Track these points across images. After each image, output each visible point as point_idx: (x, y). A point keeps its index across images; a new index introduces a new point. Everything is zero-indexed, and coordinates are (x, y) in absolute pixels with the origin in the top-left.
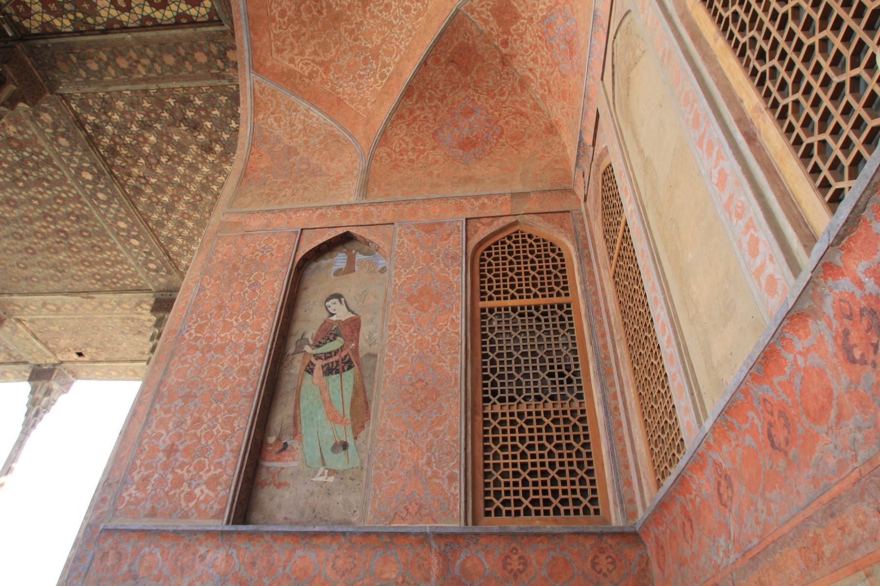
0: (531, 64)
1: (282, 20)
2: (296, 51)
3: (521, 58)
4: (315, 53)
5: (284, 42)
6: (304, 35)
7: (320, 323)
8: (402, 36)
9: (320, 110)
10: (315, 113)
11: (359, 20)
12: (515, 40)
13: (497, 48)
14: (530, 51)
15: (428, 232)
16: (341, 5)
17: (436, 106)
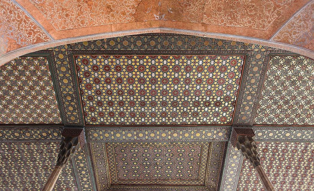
1: (252, 23)
2: (266, 20)
4: (269, 11)
6: (260, 15)
9: (298, 11)
10: (297, 15)
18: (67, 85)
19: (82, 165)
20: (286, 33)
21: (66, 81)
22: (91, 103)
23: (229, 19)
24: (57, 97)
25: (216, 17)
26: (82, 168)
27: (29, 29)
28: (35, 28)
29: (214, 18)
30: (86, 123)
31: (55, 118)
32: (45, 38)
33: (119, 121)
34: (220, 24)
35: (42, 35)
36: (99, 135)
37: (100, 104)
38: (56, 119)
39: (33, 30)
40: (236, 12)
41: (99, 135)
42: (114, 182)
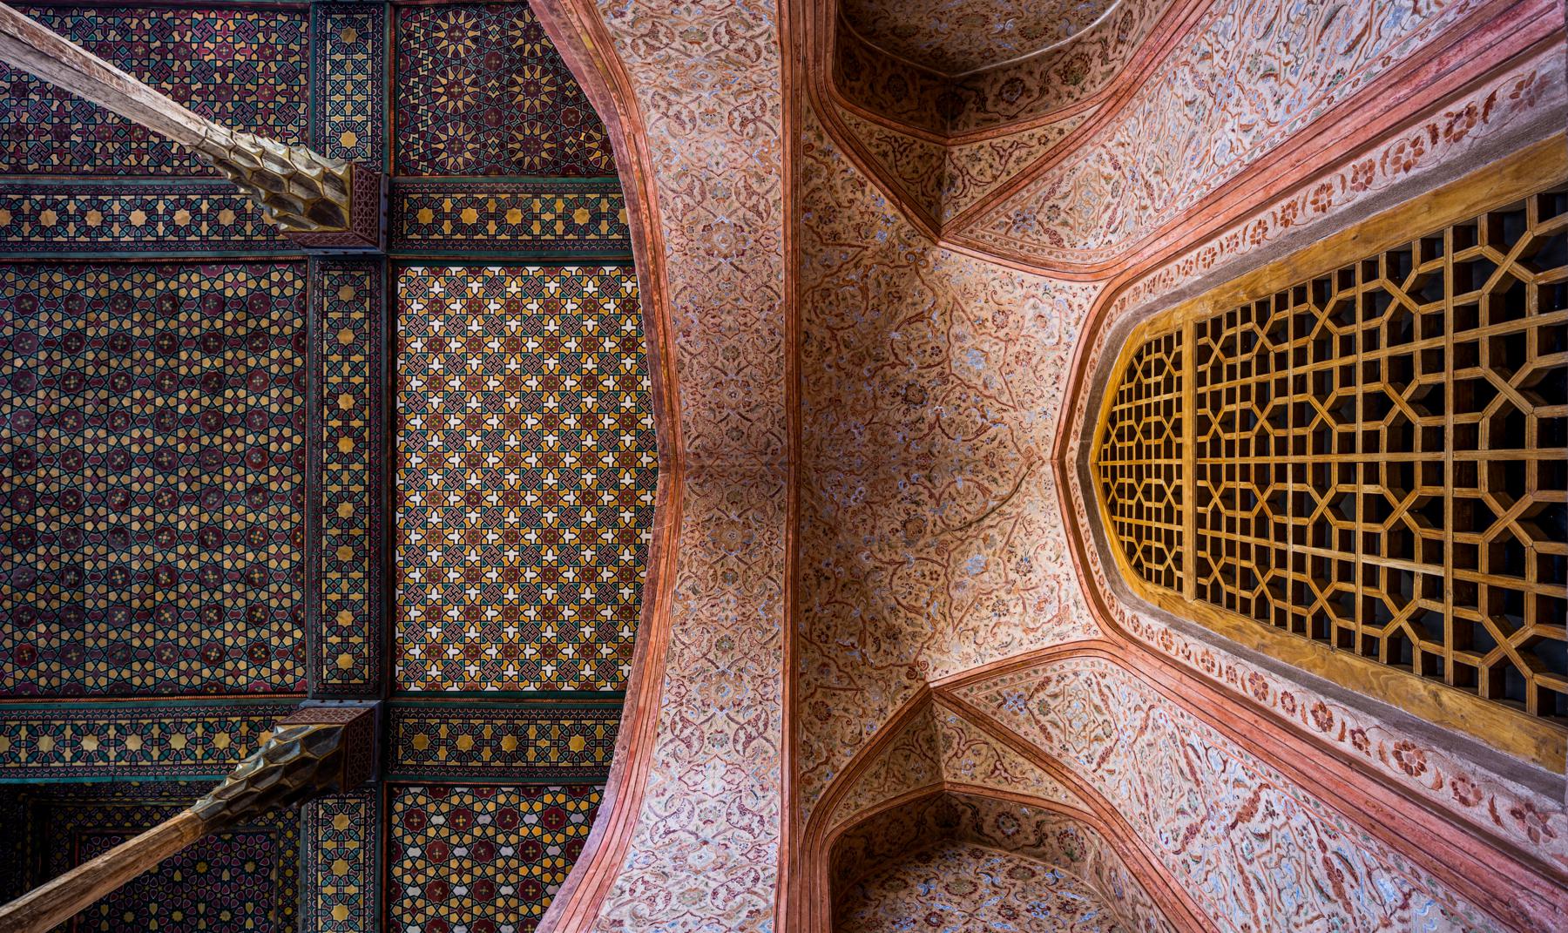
18: (561, 745)
19: (178, 742)
21: (576, 744)
22: (488, 819)
24: (510, 696)
26: (162, 742)
30: (400, 786)
31: (422, 666)
33: (407, 918)
36: (339, 837)
37: (486, 850)
38: (417, 671)
41: (339, 837)
42: (60, 817)
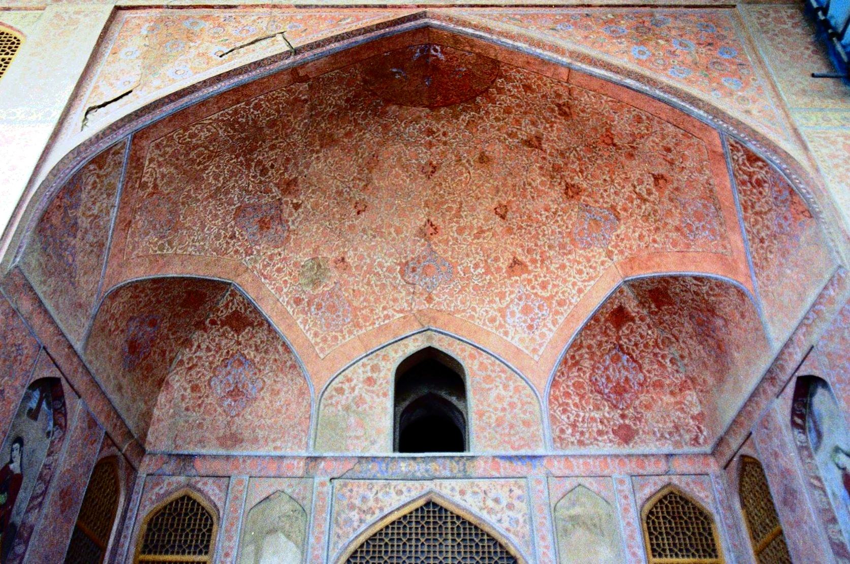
0: (203, 346)
2: (161, 159)
3: (206, 336)
4: (163, 176)
5: (167, 146)
6: (178, 159)
7: (3, 465)
8: (197, 244)
10: (114, 213)
11: (200, 197)
12: (218, 330)
13: (208, 317)
14: (214, 344)
15: (90, 427)
16: (208, 177)
17: (152, 302)
20: (110, 169)
23: (243, 117)
25: (275, 107)
27: (755, 191)
28: (743, 183)
29: (281, 103)
32: (738, 151)
34: (262, 97)
35: (740, 160)
39: (751, 183)
40: (232, 137)
